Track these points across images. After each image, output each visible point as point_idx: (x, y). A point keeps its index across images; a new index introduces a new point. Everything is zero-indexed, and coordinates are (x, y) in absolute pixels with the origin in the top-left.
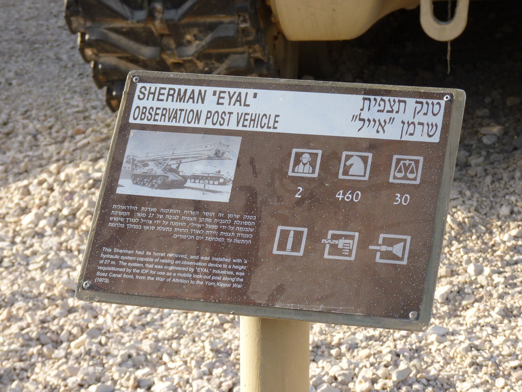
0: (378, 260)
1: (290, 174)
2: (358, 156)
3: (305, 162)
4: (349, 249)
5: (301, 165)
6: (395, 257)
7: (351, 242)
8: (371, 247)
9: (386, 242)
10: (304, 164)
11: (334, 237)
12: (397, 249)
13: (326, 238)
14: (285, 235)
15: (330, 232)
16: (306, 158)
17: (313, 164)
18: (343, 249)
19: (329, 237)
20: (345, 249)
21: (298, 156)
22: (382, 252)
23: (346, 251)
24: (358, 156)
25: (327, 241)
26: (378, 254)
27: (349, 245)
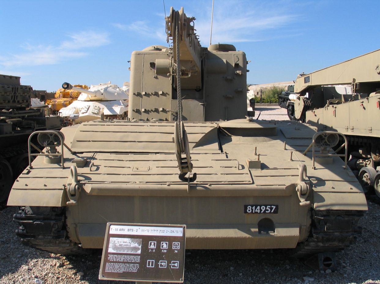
0: (172, 267)
1: (149, 248)
2: (165, 243)
6: (175, 267)
8: (170, 264)
9: (173, 263)
11: (161, 262)
12: (176, 265)
13: (159, 262)
15: (160, 261)
16: (153, 244)
21: (151, 243)
24: (165, 243)
26: (172, 266)
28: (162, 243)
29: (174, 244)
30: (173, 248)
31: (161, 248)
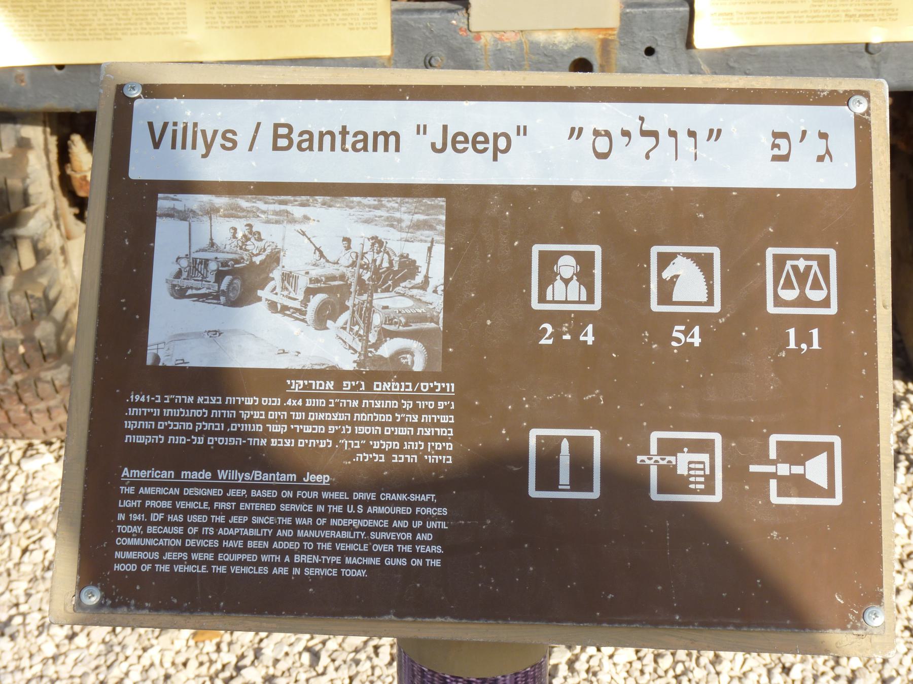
0: (775, 499)
3: (567, 276)
4: (704, 476)
7: (705, 457)
8: (753, 468)
10: (567, 282)
12: (816, 470)
13: (646, 452)
15: (655, 436)
16: (567, 266)
17: (585, 276)
18: (690, 476)
19: (654, 449)
20: (696, 476)
22: (781, 479)
23: (698, 479)
26: (773, 483)
27: (701, 466)
28: (665, 260)
29: (780, 261)
30: (771, 309)
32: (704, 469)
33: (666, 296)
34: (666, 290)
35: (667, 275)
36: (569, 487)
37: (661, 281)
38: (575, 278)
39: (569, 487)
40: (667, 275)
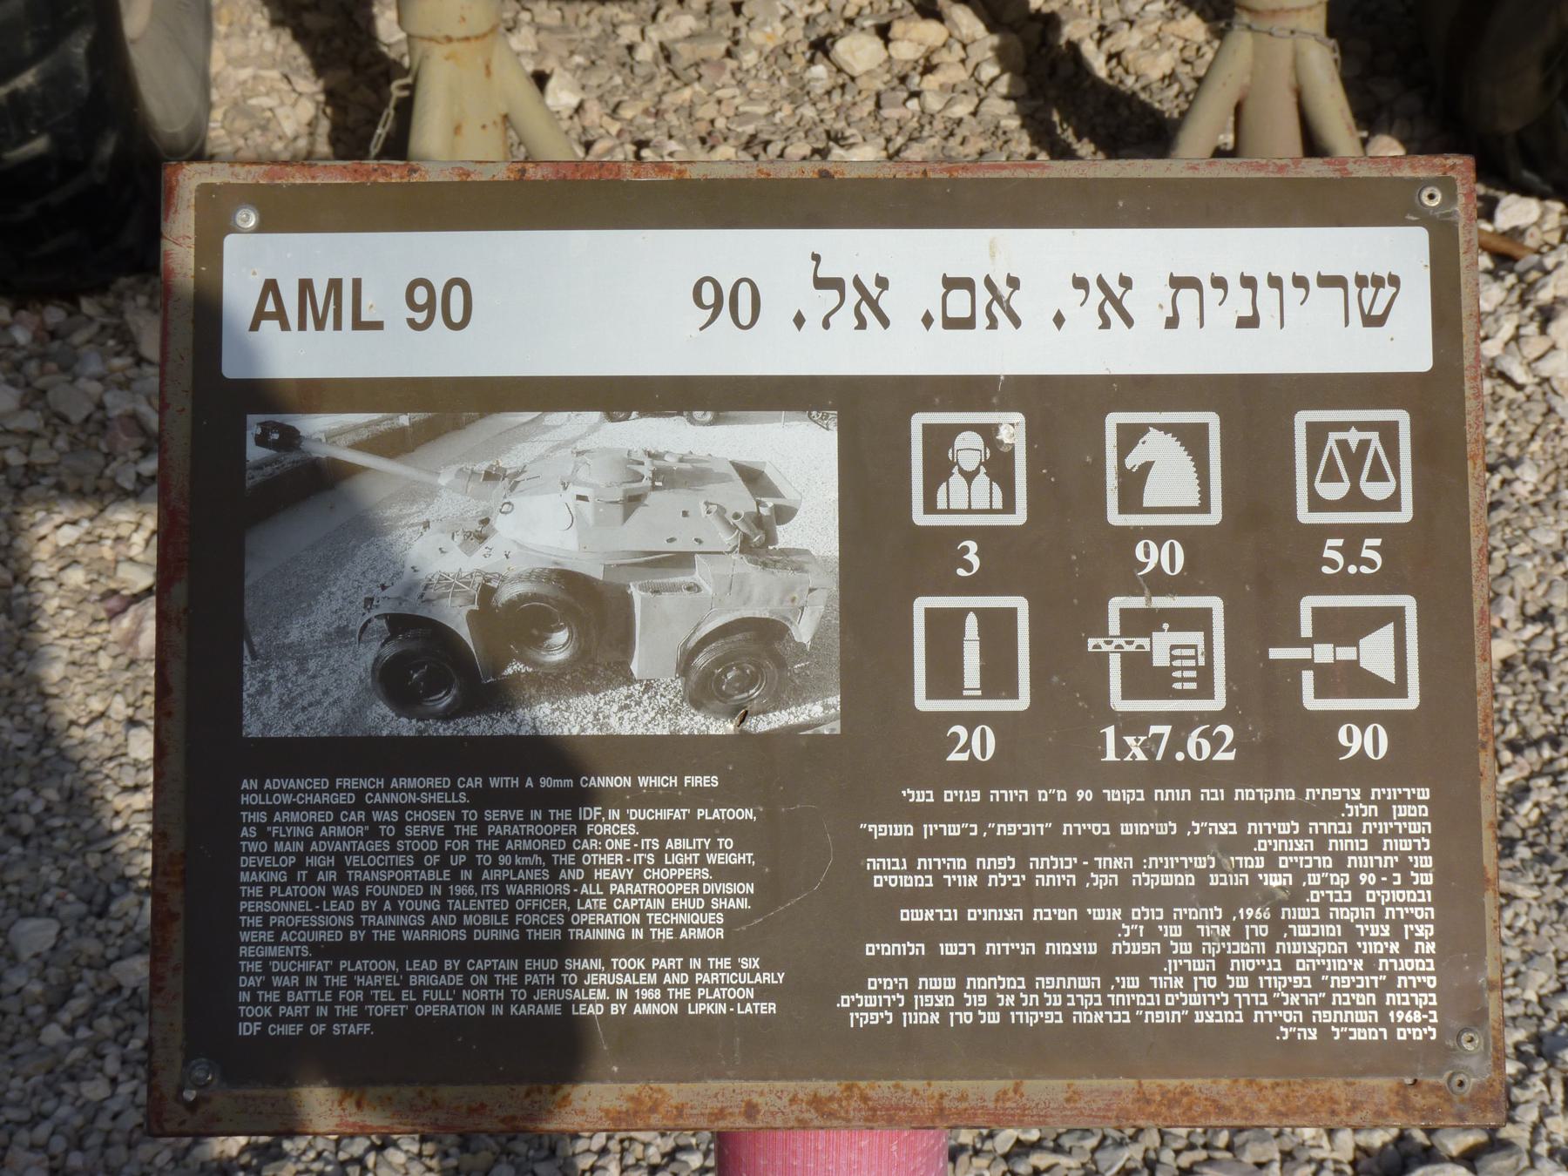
4: (1196, 668)
5: (957, 480)
10: (969, 477)
14: (945, 628)
17: (999, 465)
25: (1112, 645)
31: (1115, 518)
32: (1195, 657)
33: (1131, 497)
34: (1133, 483)
35: (1133, 461)
36: (979, 693)
37: (1122, 470)
38: (983, 469)
39: (979, 693)
40: (1133, 461)
